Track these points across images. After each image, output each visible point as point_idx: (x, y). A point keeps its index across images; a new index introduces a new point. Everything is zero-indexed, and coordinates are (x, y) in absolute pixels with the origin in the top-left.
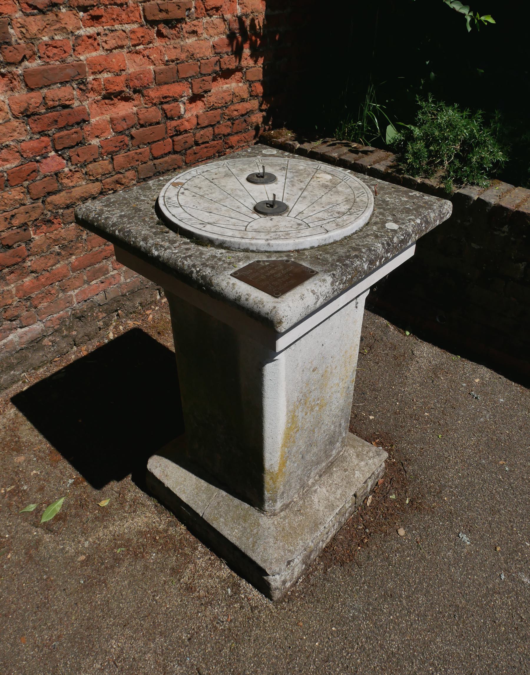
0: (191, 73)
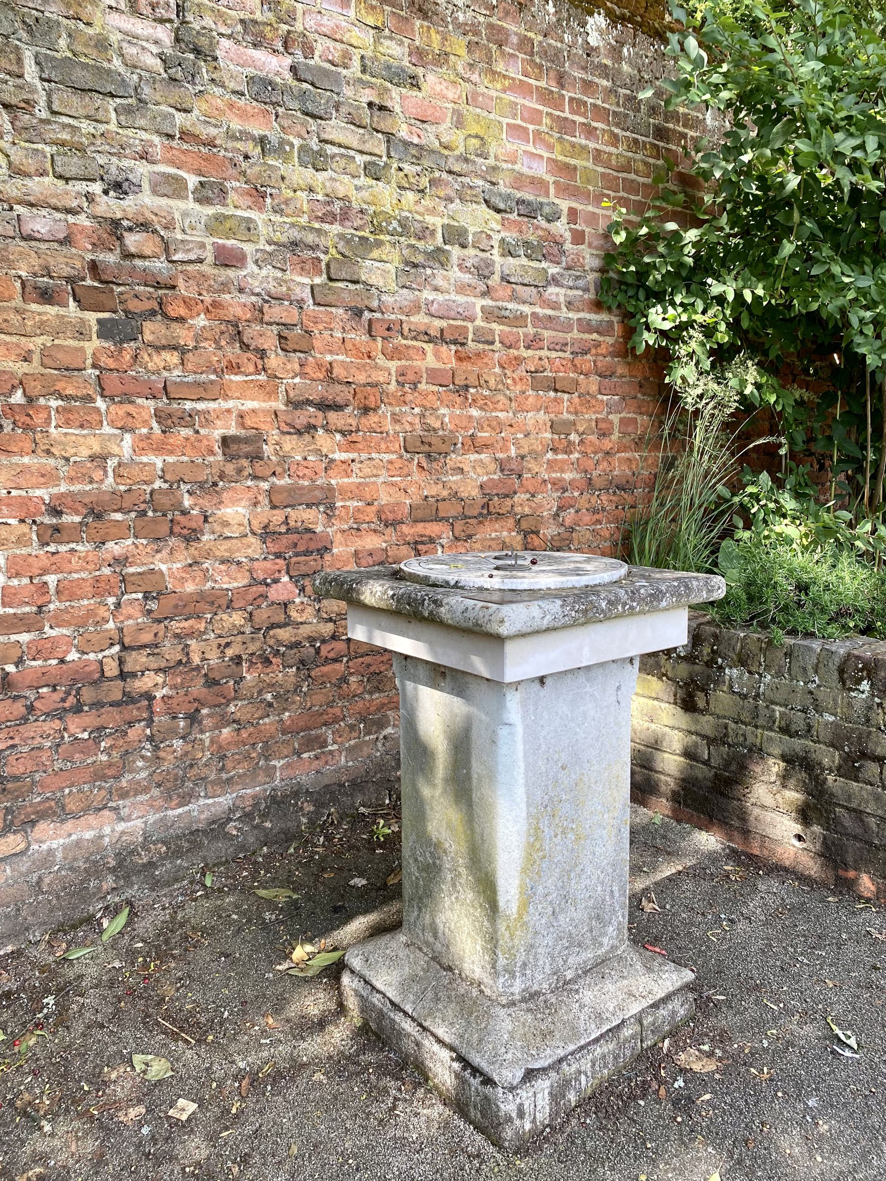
0: (453, 513)
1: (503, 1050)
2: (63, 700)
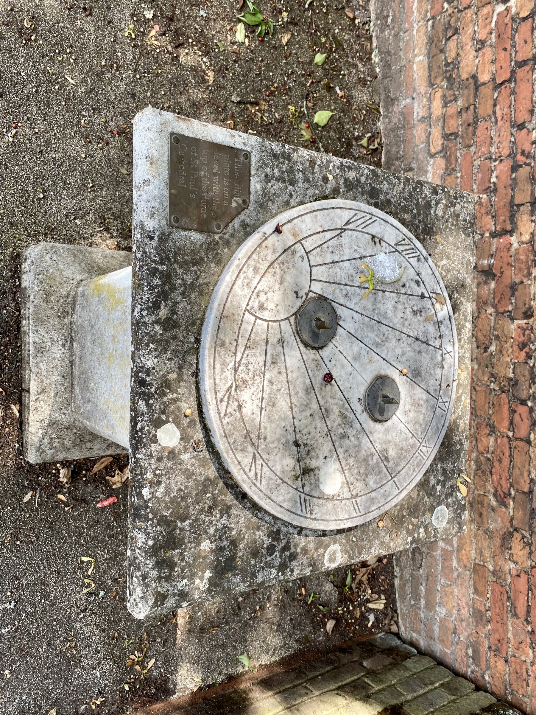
1: (54, 258)
2: (523, 153)
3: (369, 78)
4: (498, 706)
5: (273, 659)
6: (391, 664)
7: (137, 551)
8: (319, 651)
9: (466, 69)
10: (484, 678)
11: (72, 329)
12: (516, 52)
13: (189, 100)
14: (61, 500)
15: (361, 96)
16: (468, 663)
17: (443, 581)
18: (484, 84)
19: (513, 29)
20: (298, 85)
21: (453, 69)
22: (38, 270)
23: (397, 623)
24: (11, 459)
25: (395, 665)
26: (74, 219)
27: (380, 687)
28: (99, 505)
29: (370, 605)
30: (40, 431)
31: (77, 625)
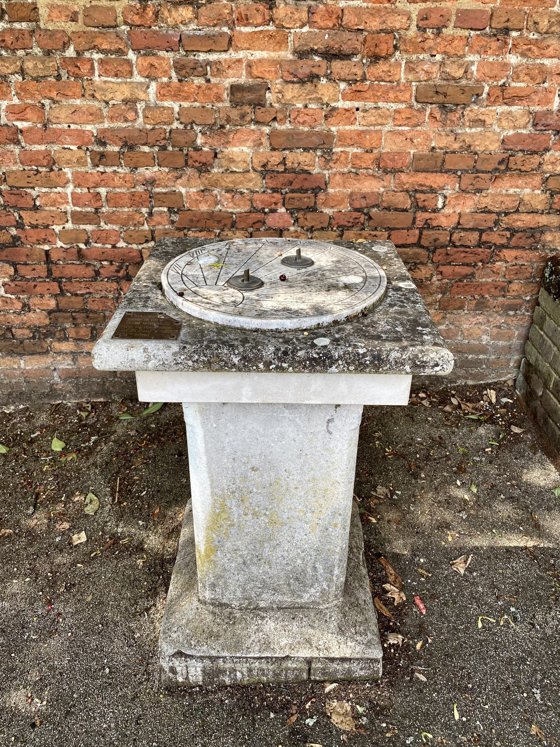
0: (462, 166)
1: (175, 629)
2: (118, 271)
3: (27, 414)
4: (545, 285)
5: (554, 469)
6: (536, 373)
7: (404, 357)
8: (541, 436)
9: (42, 320)
10: (529, 301)
11: (247, 609)
12: (40, 277)
13: (26, 548)
14: (421, 647)
15: (43, 418)
16: (521, 315)
17: (459, 338)
18: (57, 305)
19: (21, 280)
20: (25, 464)
21: (39, 332)
22: (186, 646)
23: (505, 382)
24: (383, 692)
25: (537, 371)
26: (134, 639)
27: (553, 373)
28: (424, 612)
29: (494, 400)
30: (349, 644)
31: (549, 632)
